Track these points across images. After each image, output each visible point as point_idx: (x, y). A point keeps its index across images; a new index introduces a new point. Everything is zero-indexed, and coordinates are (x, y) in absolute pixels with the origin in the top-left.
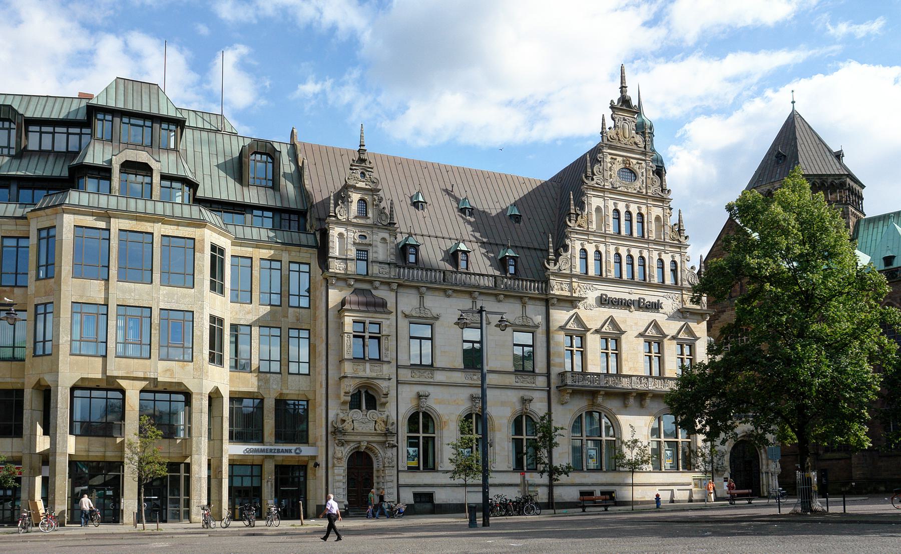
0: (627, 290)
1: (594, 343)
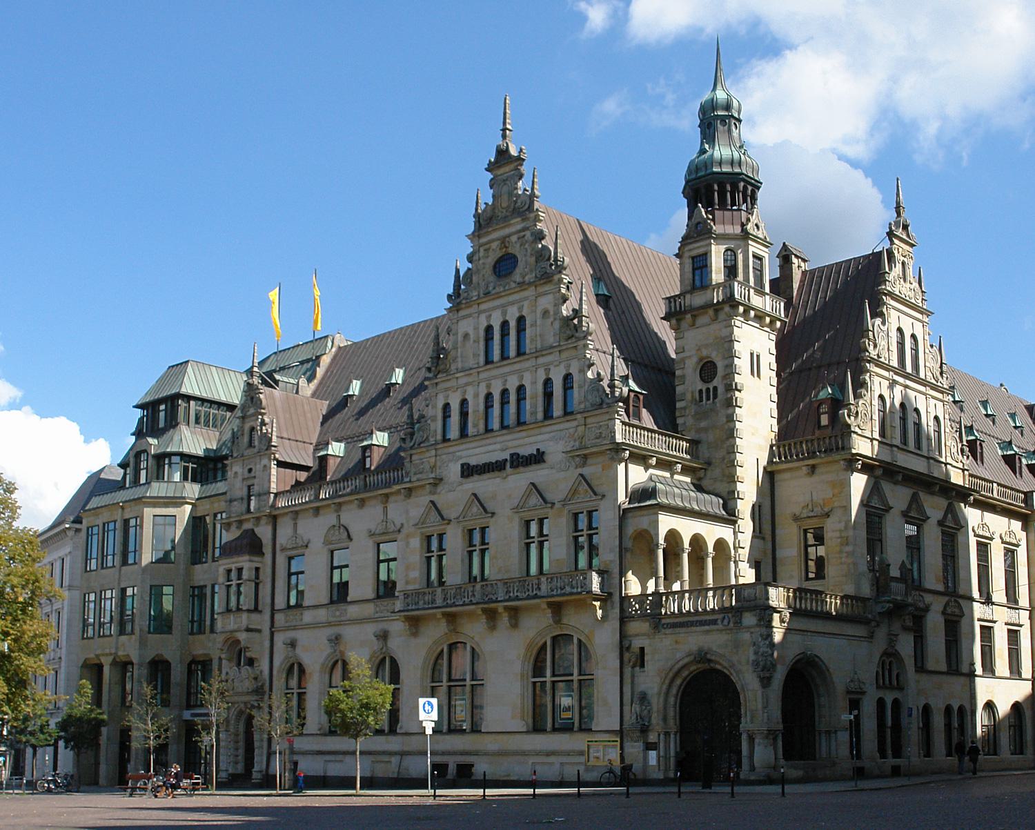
0: (498, 446)
1: (454, 540)
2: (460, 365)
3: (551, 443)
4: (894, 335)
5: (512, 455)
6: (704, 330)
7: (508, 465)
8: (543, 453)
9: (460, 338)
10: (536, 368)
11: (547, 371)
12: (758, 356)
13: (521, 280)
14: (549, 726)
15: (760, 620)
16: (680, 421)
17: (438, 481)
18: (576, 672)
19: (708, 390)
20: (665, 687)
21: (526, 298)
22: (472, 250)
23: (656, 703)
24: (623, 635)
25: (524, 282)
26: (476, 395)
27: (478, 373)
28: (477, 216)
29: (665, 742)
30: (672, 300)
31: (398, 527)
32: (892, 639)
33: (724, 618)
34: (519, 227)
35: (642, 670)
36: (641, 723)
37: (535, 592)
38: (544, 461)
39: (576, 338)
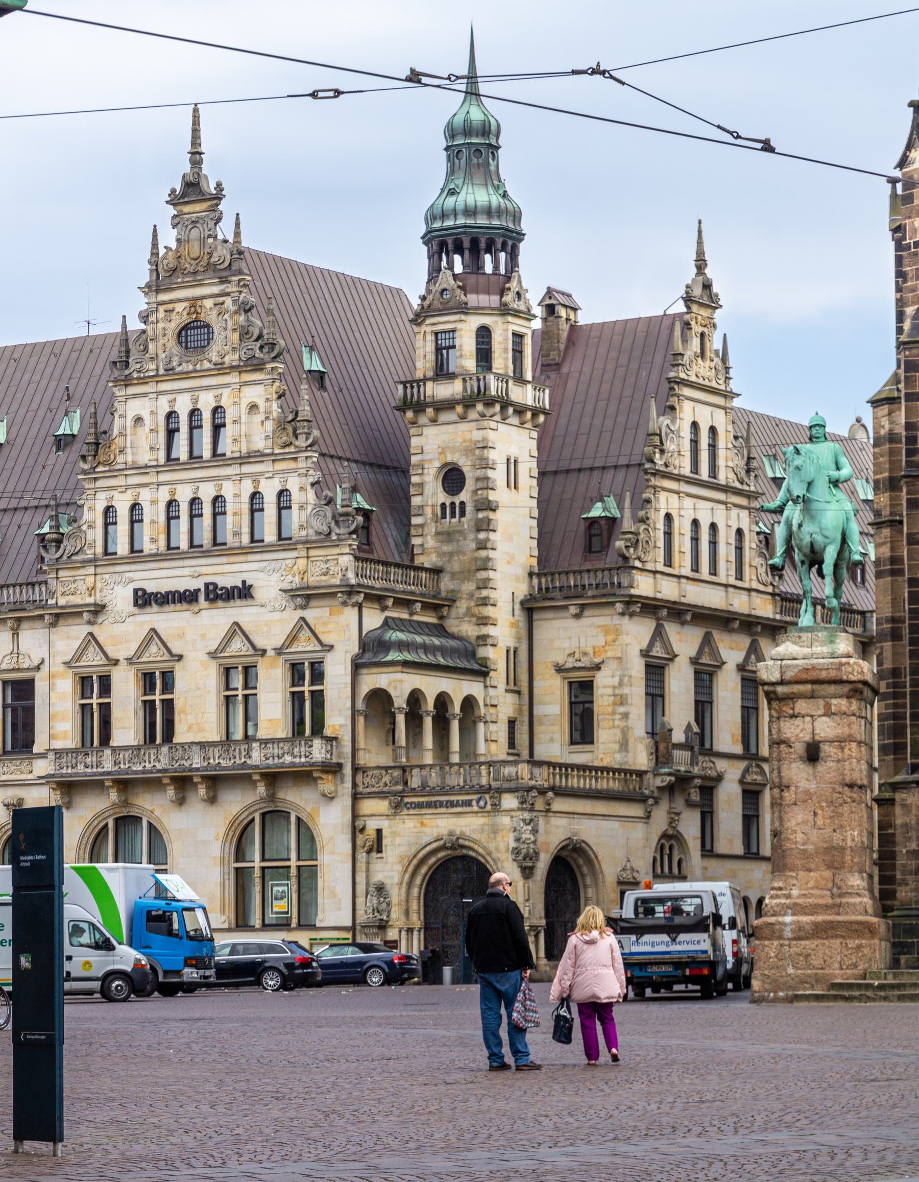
0: (187, 571)
2: (129, 459)
3: (262, 575)
4: (686, 433)
5: (207, 585)
6: (450, 428)
7: (202, 597)
8: (251, 586)
9: (129, 423)
10: (242, 477)
11: (256, 482)
12: (515, 461)
13: (220, 361)
14: (257, 923)
15: (522, 803)
16: (416, 541)
17: (98, 610)
18: (293, 855)
19: (453, 504)
20: (407, 876)
21: (226, 385)
22: (146, 307)
23: (396, 895)
24: (355, 816)
25: (223, 363)
26: (154, 502)
27: (158, 472)
28: (155, 261)
29: (408, 940)
30: (408, 385)
31: (36, 663)
32: (674, 817)
33: (480, 798)
34: (216, 290)
35: (379, 855)
36: (379, 917)
37: (243, 760)
38: (252, 597)
39: (296, 447)
